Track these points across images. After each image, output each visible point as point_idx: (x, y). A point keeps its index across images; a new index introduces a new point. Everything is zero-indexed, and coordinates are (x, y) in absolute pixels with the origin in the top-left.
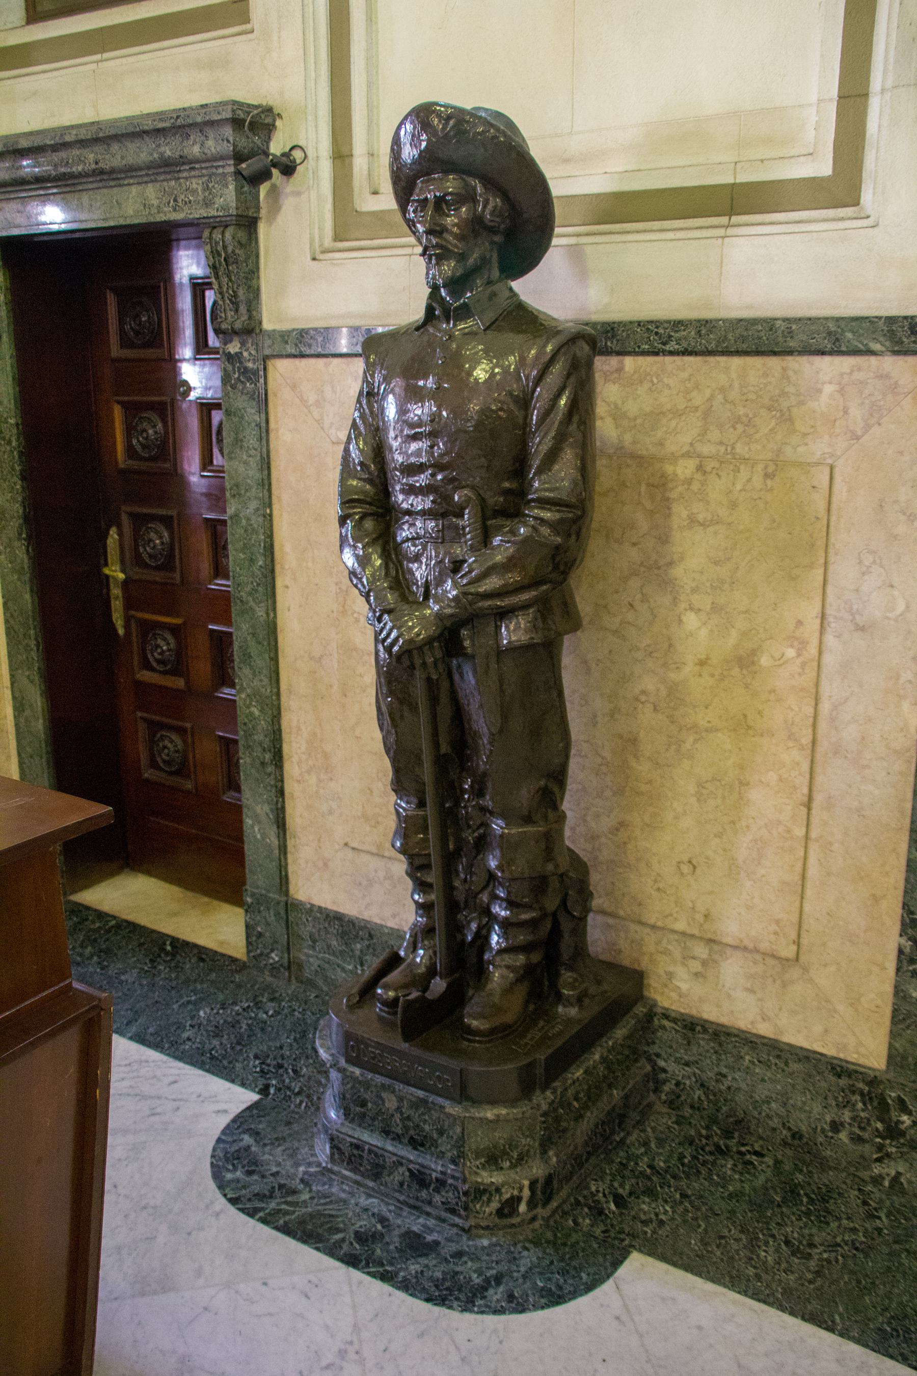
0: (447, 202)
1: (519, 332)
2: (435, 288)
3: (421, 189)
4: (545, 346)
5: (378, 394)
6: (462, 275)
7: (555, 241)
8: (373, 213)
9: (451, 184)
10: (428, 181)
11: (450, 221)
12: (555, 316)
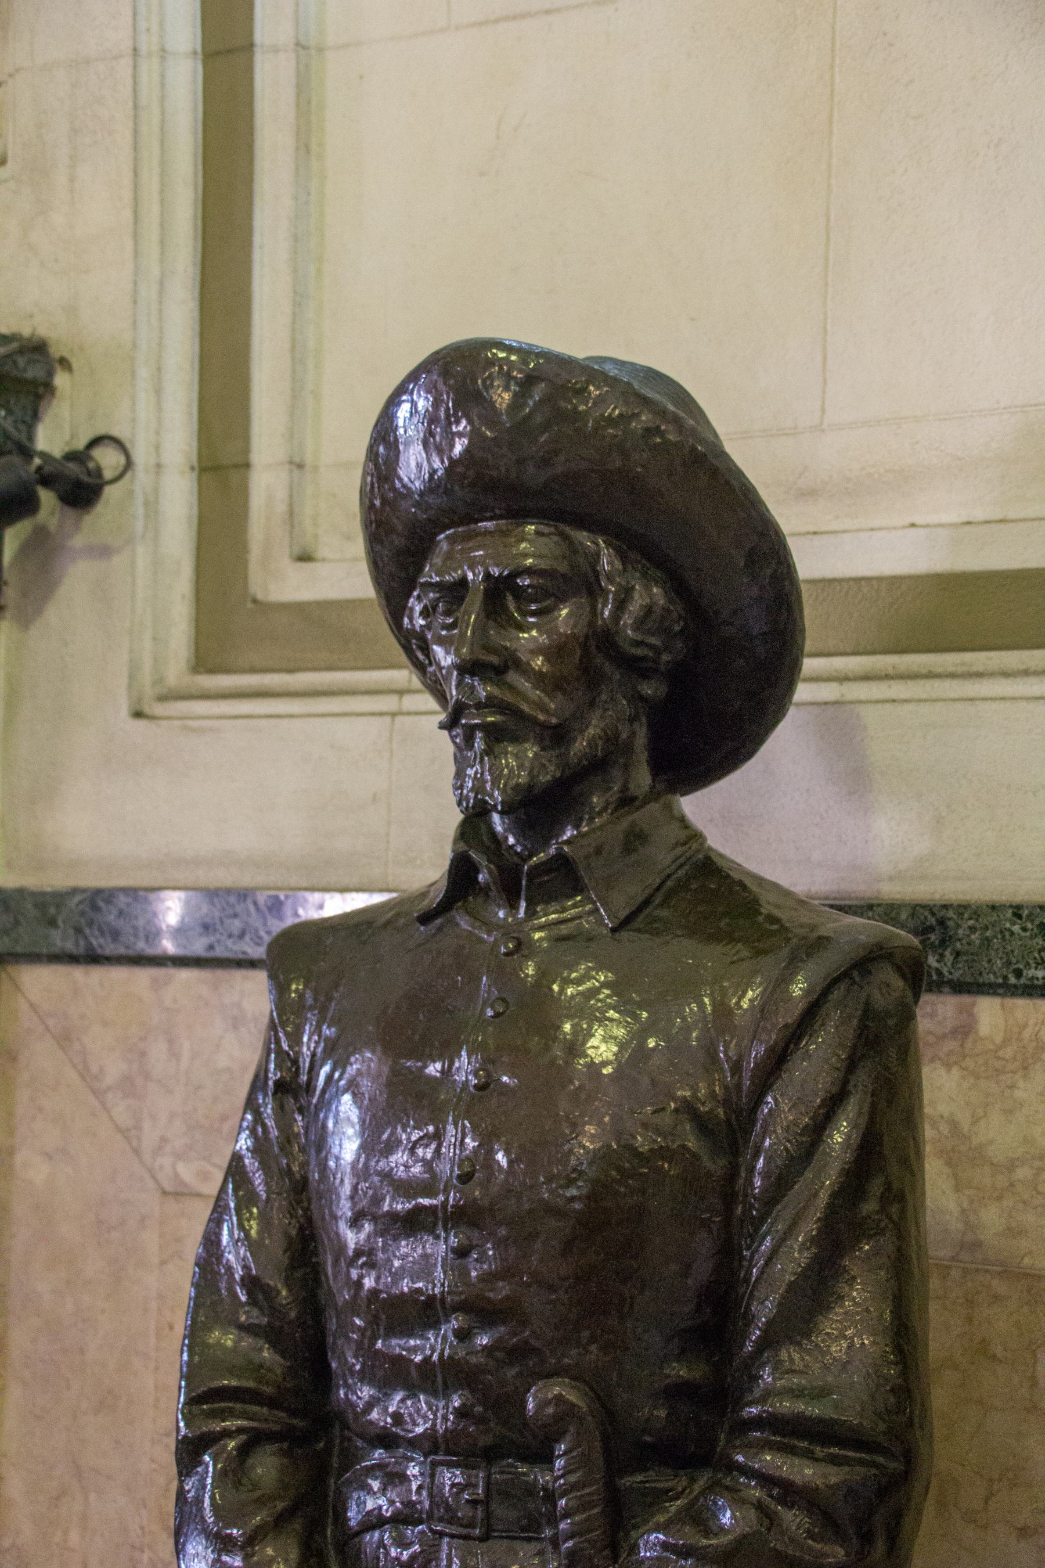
0: (519, 593)
2: (476, 817)
3: (449, 556)
4: (785, 980)
7: (802, 692)
8: (300, 609)
9: (531, 546)
10: (468, 537)
11: (530, 637)
12: (784, 882)
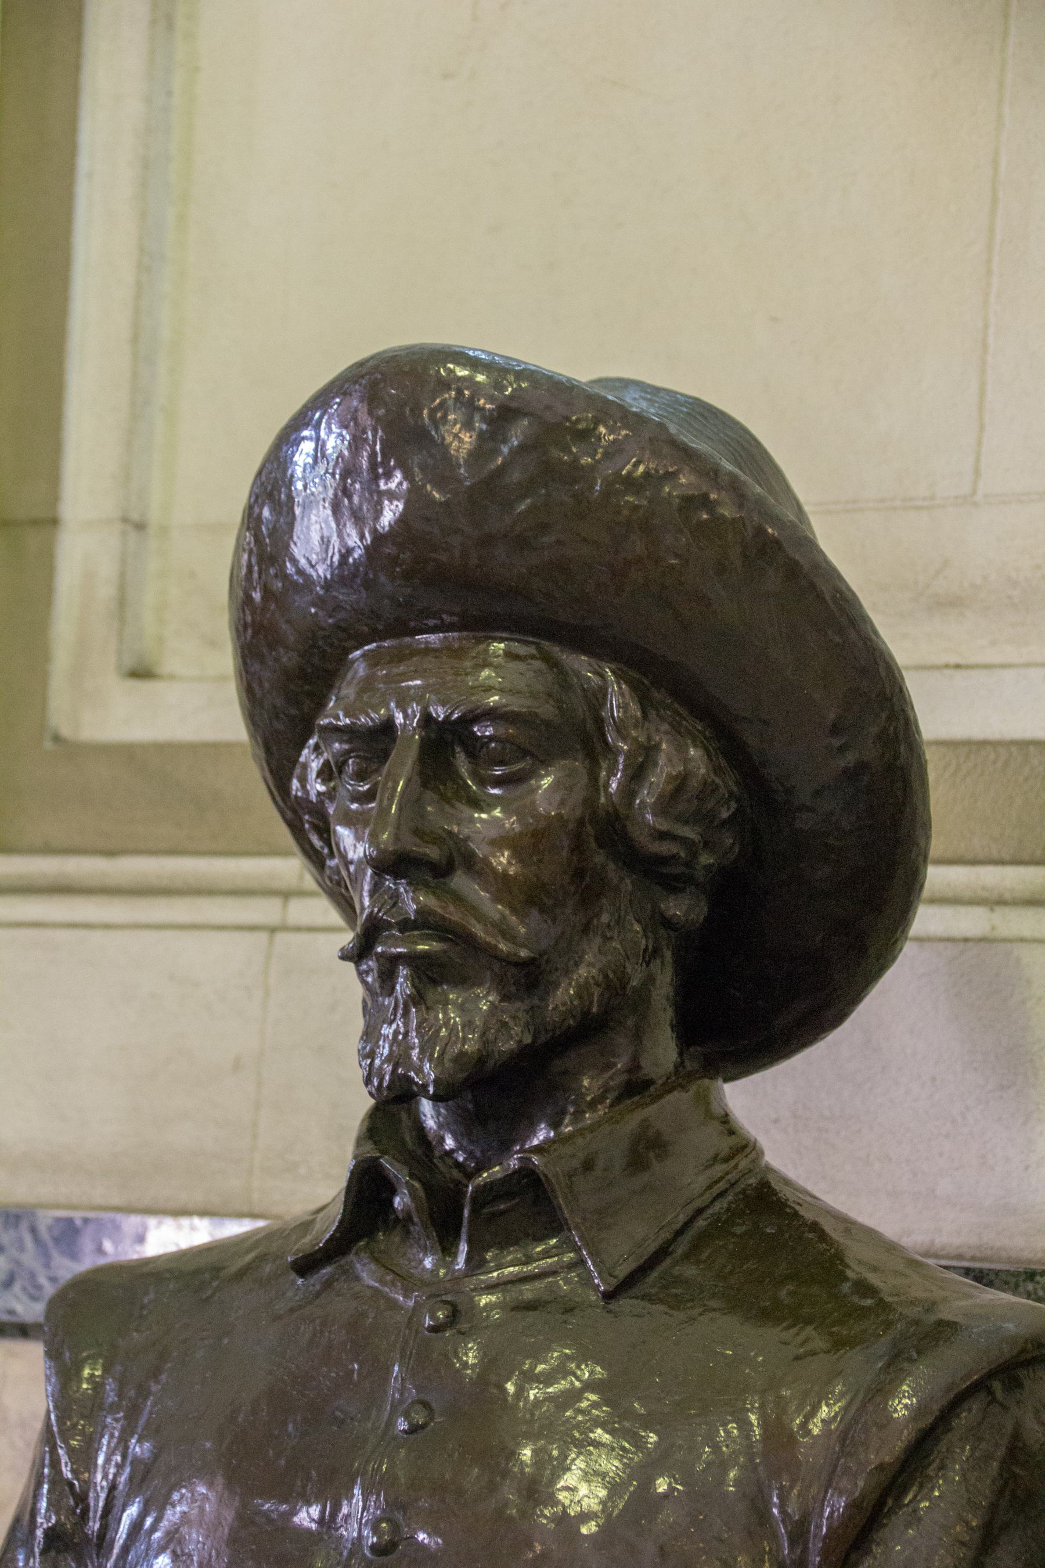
0: (474, 748)
1: (766, 1315)
2: (393, 1102)
3: (367, 686)
4: (881, 1390)
5: (103, 1541)
6: (523, 1053)
7: (926, 920)
8: (128, 754)
9: (498, 675)
10: (398, 657)
11: (488, 822)
